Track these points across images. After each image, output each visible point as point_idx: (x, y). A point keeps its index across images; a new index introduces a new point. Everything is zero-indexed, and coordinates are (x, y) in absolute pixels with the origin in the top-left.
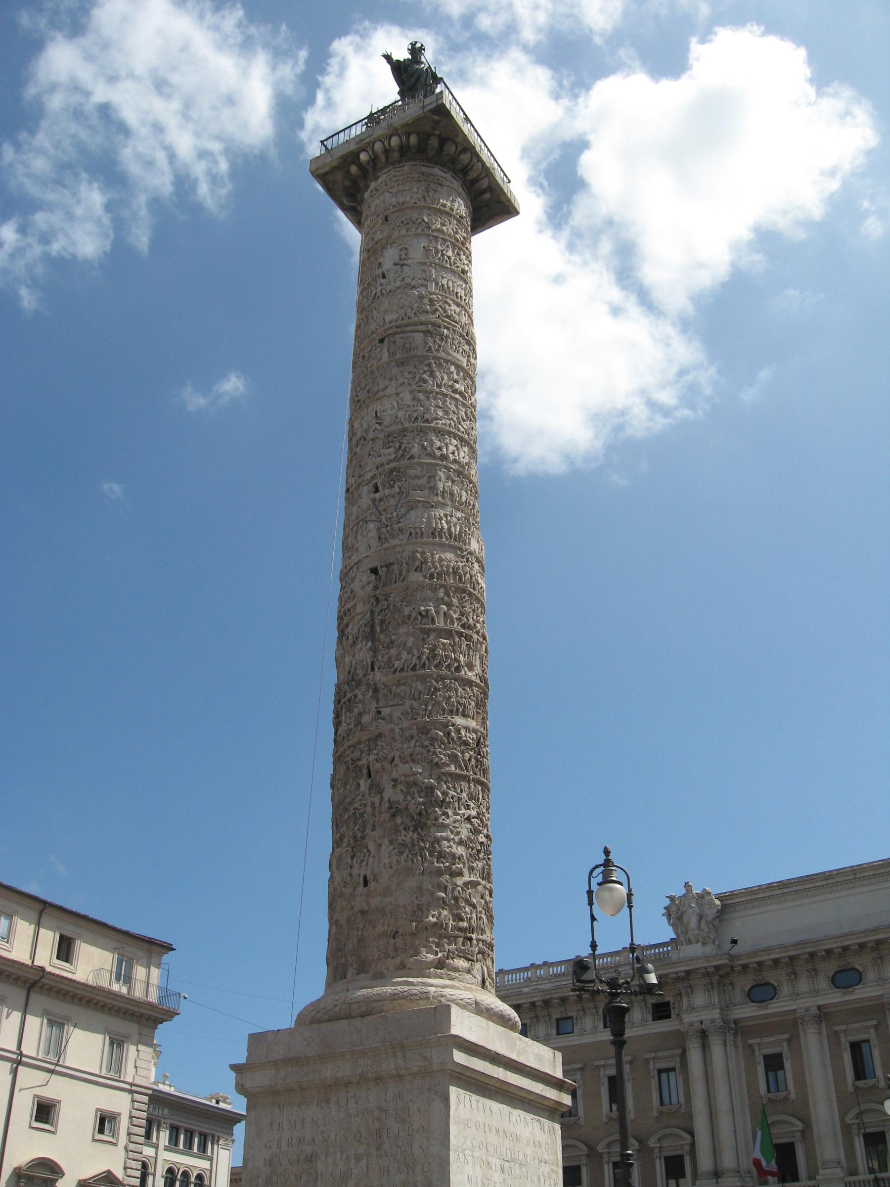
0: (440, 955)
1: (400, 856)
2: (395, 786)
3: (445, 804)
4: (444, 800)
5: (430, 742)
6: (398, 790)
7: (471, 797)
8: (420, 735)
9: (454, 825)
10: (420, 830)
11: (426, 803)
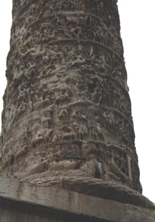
0: (45, 161)
1: (18, 109)
2: (19, 69)
3: (51, 61)
4: (50, 59)
5: (41, 32)
6: (20, 70)
7: (77, 52)
8: (34, 31)
9: (61, 71)
10: (31, 85)
11: (36, 66)
